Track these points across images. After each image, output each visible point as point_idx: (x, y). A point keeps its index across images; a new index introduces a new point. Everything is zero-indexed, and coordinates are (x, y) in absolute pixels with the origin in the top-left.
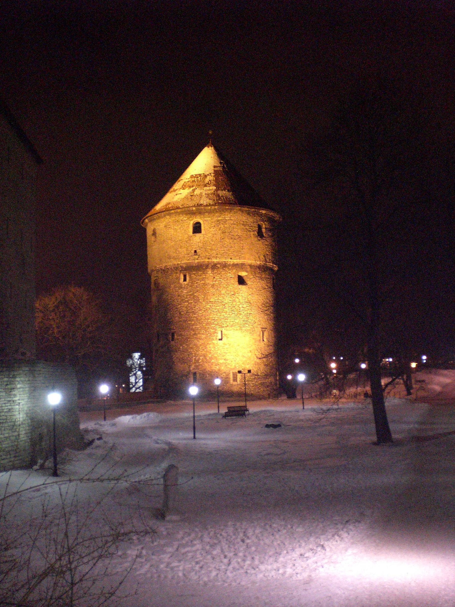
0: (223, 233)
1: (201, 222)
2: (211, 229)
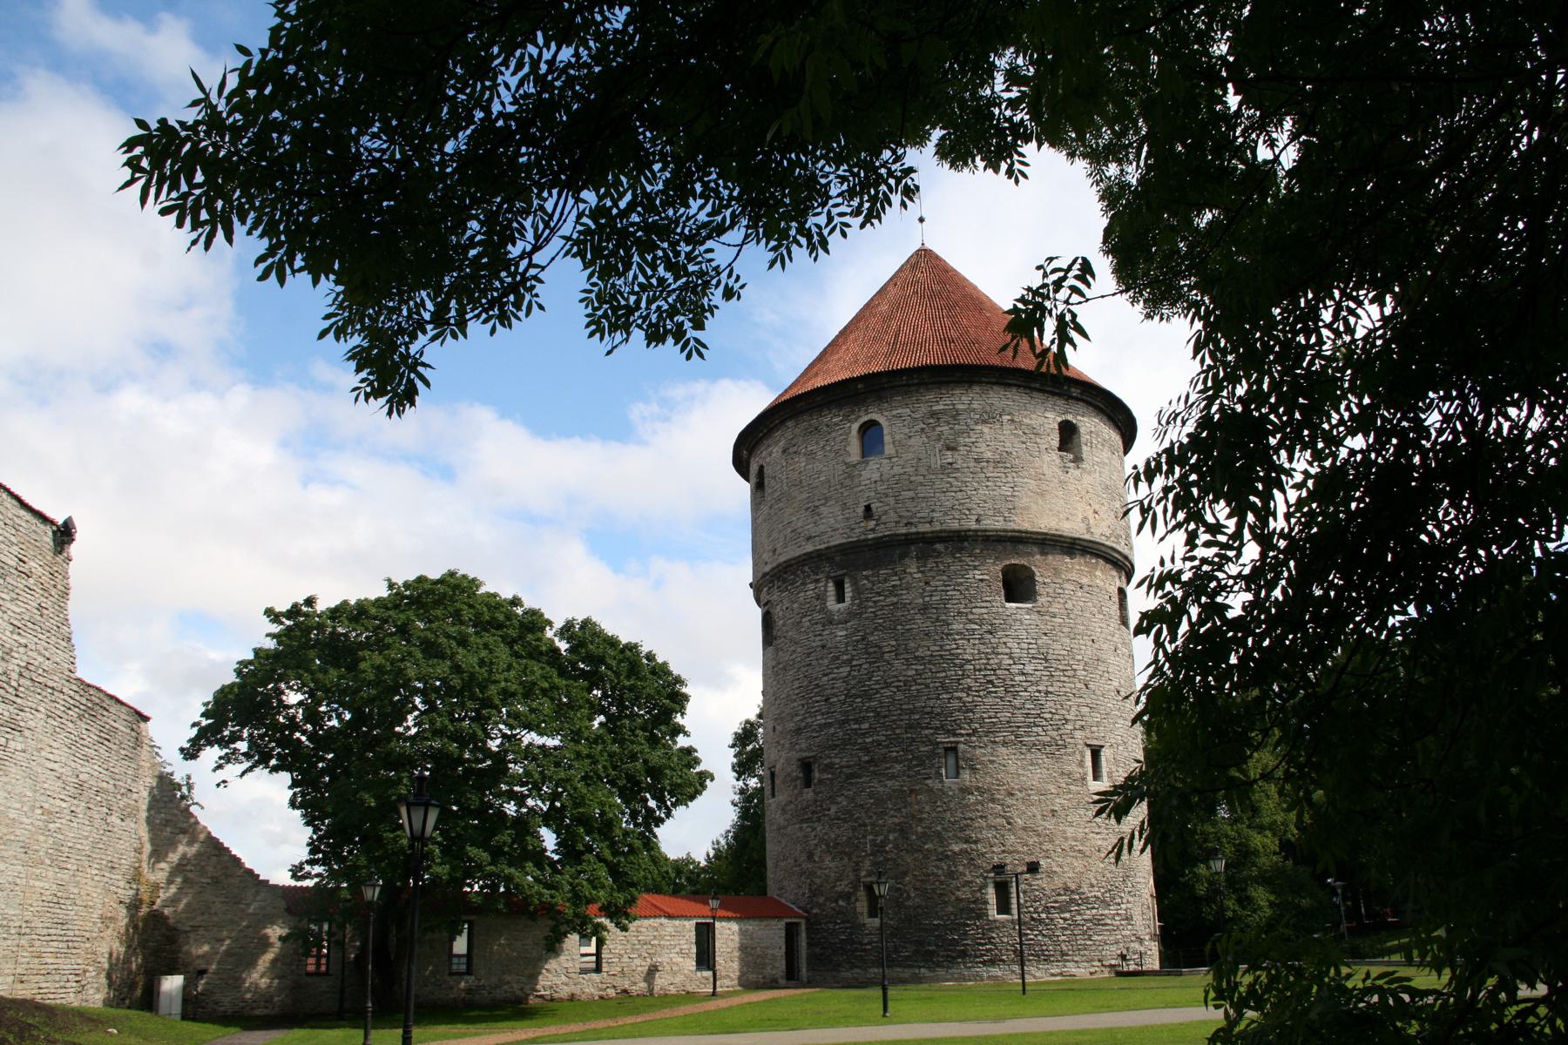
0: (949, 449)
1: (882, 420)
2: (912, 441)
